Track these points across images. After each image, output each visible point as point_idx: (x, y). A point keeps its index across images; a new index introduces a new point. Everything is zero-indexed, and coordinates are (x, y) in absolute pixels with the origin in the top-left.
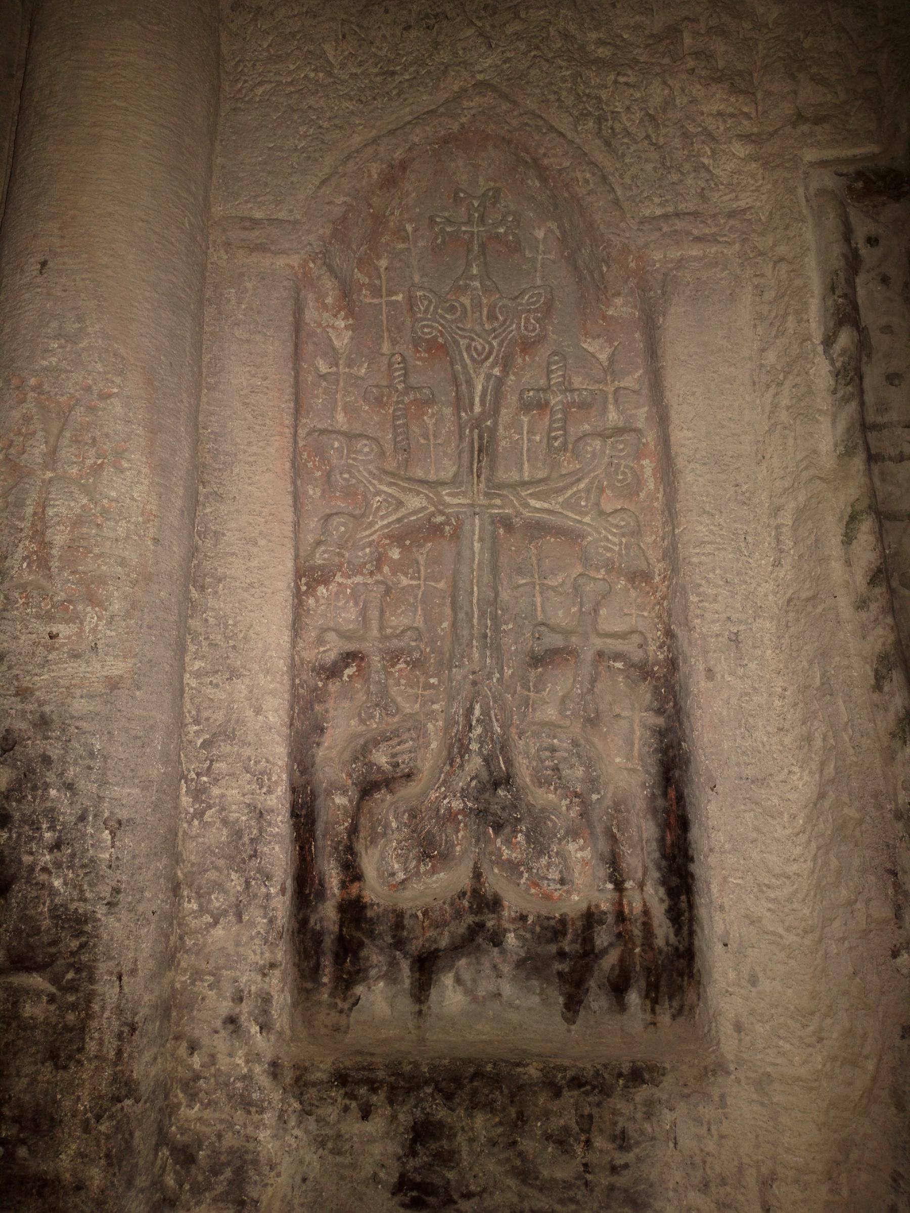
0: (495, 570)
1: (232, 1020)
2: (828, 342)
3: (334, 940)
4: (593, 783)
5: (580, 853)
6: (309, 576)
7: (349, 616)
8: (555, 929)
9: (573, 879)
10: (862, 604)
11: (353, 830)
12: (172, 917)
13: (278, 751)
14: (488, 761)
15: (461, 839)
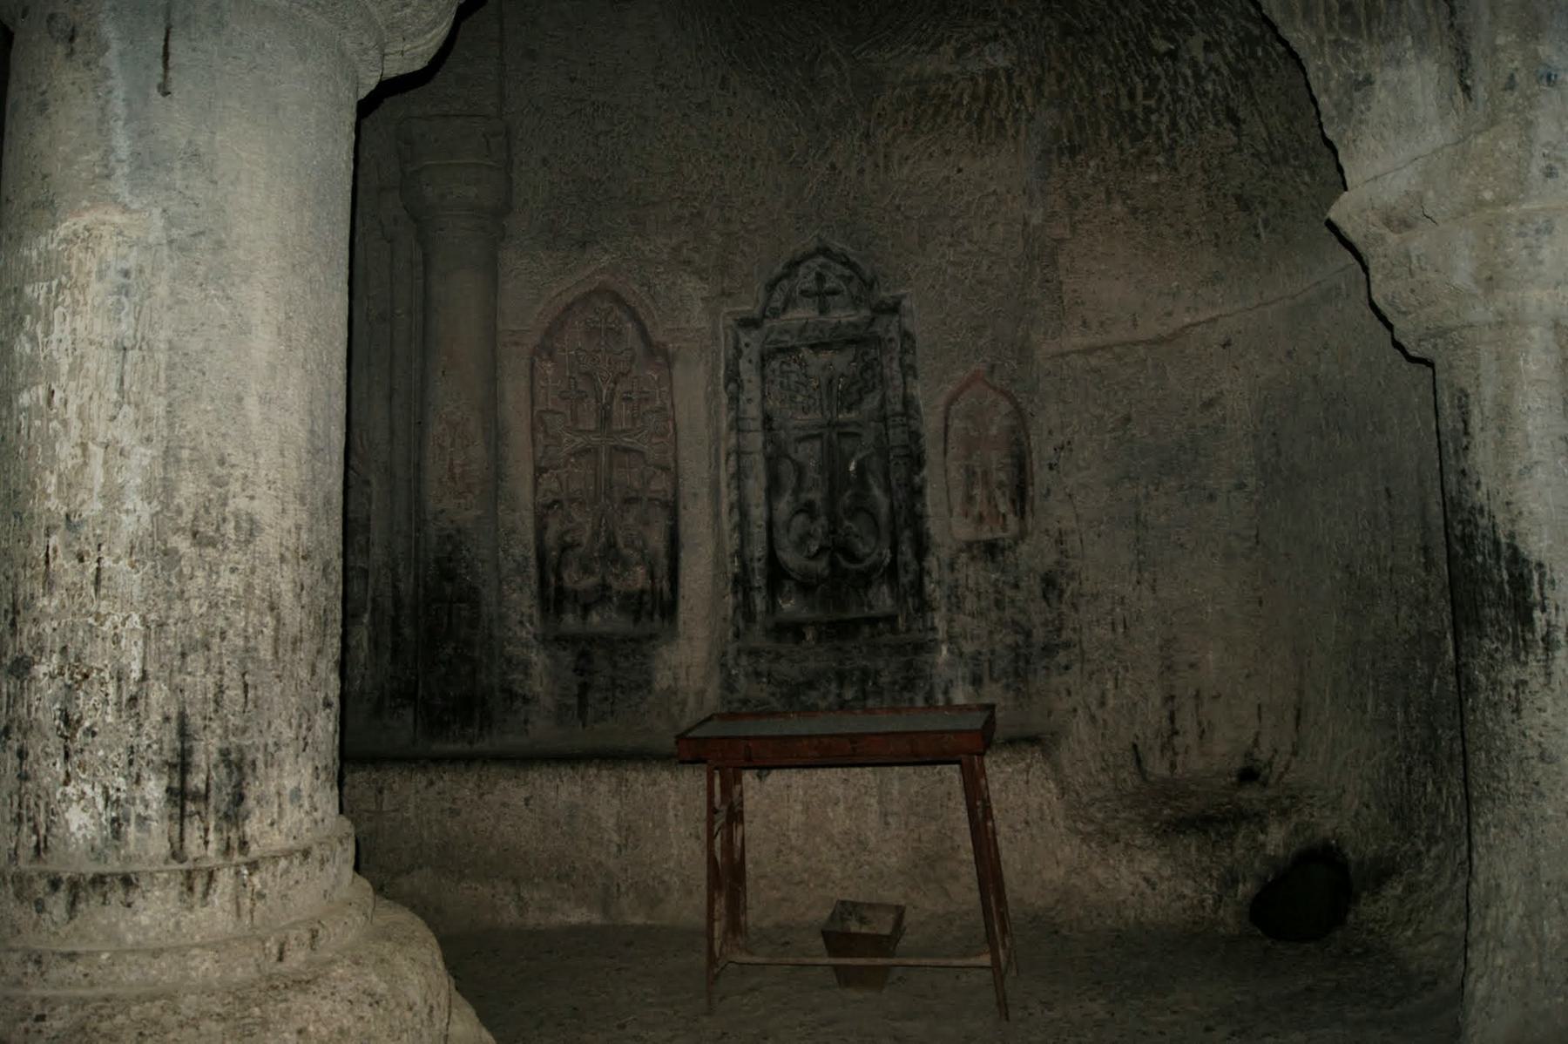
0: (611, 466)
1: (521, 623)
2: (726, 387)
3: (553, 599)
4: (645, 545)
5: (640, 571)
6: (539, 471)
7: (555, 486)
8: (628, 596)
9: (638, 578)
10: (728, 486)
11: (559, 564)
12: (499, 590)
13: (530, 537)
14: (608, 539)
15: (597, 567)
